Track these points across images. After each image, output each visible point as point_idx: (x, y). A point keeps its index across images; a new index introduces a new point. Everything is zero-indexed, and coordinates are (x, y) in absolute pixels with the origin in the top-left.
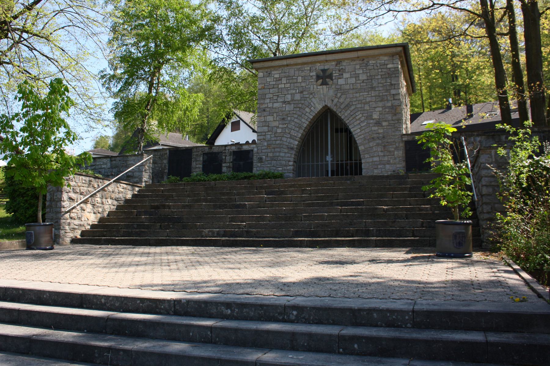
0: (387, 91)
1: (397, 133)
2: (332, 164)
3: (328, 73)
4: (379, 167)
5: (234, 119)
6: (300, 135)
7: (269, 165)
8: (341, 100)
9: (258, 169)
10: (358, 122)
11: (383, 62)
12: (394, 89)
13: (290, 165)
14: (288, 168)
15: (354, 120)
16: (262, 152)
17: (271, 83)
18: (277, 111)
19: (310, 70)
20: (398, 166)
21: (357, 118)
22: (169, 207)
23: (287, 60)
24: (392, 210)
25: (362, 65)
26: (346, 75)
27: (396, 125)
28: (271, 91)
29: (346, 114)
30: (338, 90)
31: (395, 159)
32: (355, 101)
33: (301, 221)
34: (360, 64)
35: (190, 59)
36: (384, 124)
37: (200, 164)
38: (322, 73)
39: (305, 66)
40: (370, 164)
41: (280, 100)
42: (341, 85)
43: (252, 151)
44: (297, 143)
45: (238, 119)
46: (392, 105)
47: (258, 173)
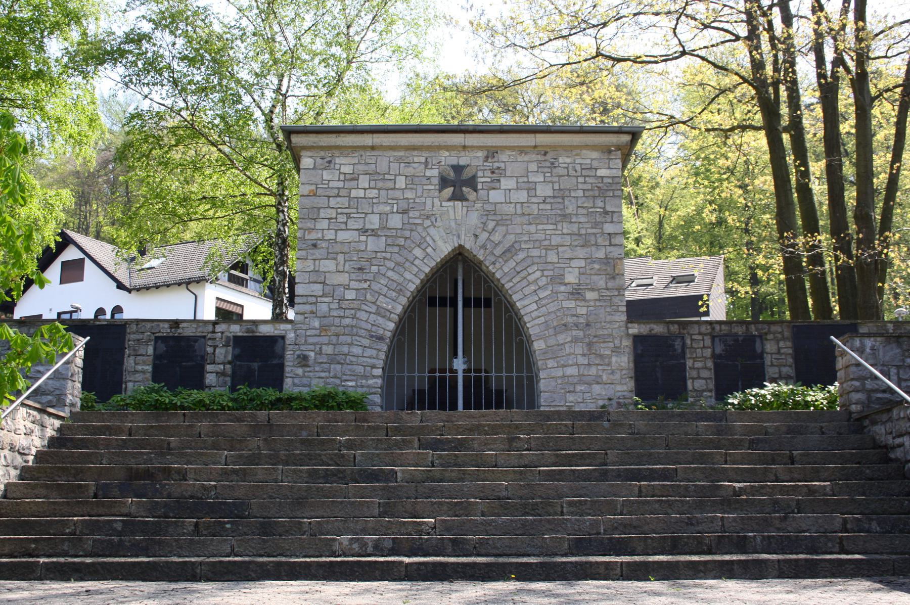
0: (596, 224)
2: (466, 380)
3: (467, 174)
4: (579, 388)
5: (71, 254)
6: (399, 309)
7: (323, 375)
8: (496, 237)
9: (296, 381)
10: (533, 287)
11: (589, 161)
12: (612, 222)
13: (374, 377)
14: (371, 382)
15: (525, 283)
16: (306, 343)
17: (332, 184)
18: (346, 249)
19: (426, 163)
20: (619, 388)
21: (531, 278)
22: (183, 475)
23: (375, 135)
24: (753, 491)
25: (544, 164)
26: (506, 183)
31: (613, 373)
33: (562, 514)
34: (539, 162)
35: (53, 106)
36: (590, 295)
37: (144, 363)
38: (452, 174)
39: (415, 153)
40: (559, 381)
41: (352, 224)
43: (283, 338)
44: (391, 326)
45: (81, 256)
46: (606, 258)
47: (296, 390)
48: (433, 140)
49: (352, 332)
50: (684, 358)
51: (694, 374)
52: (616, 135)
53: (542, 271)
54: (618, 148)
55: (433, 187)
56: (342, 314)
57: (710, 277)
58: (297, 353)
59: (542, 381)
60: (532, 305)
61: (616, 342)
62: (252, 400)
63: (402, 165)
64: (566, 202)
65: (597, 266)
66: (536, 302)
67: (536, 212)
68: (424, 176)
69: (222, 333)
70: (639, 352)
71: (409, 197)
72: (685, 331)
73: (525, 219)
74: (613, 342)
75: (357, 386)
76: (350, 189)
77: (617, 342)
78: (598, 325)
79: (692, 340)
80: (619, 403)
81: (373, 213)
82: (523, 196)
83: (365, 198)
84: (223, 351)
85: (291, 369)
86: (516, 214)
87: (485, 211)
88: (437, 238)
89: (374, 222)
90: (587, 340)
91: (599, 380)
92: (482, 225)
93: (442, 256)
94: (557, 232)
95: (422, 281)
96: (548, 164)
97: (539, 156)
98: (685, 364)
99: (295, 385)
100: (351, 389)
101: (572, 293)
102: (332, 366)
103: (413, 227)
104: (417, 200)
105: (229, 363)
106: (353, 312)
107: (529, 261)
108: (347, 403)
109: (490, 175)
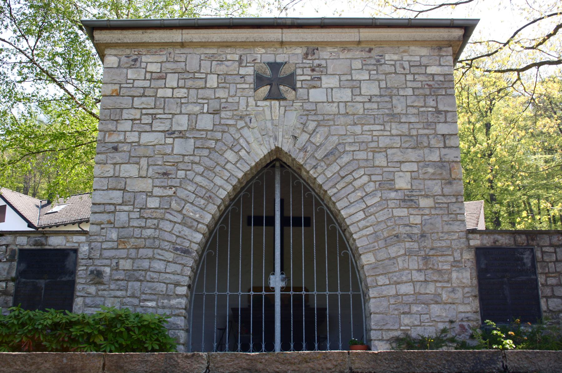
0: (428, 125)
1: (455, 228)
2: (285, 300)
3: (284, 72)
4: (415, 309)
6: (208, 218)
7: (119, 293)
8: (318, 139)
9: (88, 301)
10: (360, 194)
11: (418, 58)
12: (446, 122)
13: (178, 296)
14: (174, 302)
15: (350, 189)
16: (101, 257)
17: (136, 84)
18: (149, 152)
19: (240, 61)
20: (461, 308)
21: (357, 183)
23: (185, 31)
25: (368, 62)
26: (327, 82)
27: (454, 207)
28: (137, 102)
29: (329, 174)
30: (307, 113)
31: (453, 291)
32: (350, 144)
34: (364, 59)
36: (424, 202)
39: (229, 50)
40: (392, 301)
41: (157, 125)
42: (316, 103)
43: (75, 251)
44: (199, 237)
45: (4, 203)
46: (441, 161)
47: (89, 311)
48: (248, 35)
49: (154, 243)
50: (535, 273)
51: (548, 292)
53: (370, 175)
54: (449, 43)
55: (247, 86)
56: (143, 224)
57: (476, 216)
58: (91, 268)
59: (372, 301)
60: (360, 214)
62: (23, 325)
63: (214, 63)
64: (394, 101)
65: (431, 170)
66: (363, 210)
67: (361, 111)
68: (238, 74)
69: (7, 246)
70: (483, 266)
71: (221, 96)
73: (349, 119)
74: (452, 255)
75: (158, 307)
76: (157, 89)
77: (457, 255)
78: (435, 236)
79: (543, 253)
80: (462, 327)
81: (181, 113)
82: (346, 95)
83: (172, 97)
85: (83, 285)
86: (339, 114)
87: (304, 110)
88: (251, 140)
89: (182, 123)
90: (423, 253)
91: (438, 299)
92: (301, 126)
93: (258, 160)
95: (234, 187)
96: (373, 62)
97: (363, 53)
98: (536, 280)
99: (86, 305)
101: (404, 201)
102: (130, 284)
103: (225, 128)
104: (230, 100)
105: (13, 280)
106: (156, 222)
107: (354, 165)
109: (310, 73)
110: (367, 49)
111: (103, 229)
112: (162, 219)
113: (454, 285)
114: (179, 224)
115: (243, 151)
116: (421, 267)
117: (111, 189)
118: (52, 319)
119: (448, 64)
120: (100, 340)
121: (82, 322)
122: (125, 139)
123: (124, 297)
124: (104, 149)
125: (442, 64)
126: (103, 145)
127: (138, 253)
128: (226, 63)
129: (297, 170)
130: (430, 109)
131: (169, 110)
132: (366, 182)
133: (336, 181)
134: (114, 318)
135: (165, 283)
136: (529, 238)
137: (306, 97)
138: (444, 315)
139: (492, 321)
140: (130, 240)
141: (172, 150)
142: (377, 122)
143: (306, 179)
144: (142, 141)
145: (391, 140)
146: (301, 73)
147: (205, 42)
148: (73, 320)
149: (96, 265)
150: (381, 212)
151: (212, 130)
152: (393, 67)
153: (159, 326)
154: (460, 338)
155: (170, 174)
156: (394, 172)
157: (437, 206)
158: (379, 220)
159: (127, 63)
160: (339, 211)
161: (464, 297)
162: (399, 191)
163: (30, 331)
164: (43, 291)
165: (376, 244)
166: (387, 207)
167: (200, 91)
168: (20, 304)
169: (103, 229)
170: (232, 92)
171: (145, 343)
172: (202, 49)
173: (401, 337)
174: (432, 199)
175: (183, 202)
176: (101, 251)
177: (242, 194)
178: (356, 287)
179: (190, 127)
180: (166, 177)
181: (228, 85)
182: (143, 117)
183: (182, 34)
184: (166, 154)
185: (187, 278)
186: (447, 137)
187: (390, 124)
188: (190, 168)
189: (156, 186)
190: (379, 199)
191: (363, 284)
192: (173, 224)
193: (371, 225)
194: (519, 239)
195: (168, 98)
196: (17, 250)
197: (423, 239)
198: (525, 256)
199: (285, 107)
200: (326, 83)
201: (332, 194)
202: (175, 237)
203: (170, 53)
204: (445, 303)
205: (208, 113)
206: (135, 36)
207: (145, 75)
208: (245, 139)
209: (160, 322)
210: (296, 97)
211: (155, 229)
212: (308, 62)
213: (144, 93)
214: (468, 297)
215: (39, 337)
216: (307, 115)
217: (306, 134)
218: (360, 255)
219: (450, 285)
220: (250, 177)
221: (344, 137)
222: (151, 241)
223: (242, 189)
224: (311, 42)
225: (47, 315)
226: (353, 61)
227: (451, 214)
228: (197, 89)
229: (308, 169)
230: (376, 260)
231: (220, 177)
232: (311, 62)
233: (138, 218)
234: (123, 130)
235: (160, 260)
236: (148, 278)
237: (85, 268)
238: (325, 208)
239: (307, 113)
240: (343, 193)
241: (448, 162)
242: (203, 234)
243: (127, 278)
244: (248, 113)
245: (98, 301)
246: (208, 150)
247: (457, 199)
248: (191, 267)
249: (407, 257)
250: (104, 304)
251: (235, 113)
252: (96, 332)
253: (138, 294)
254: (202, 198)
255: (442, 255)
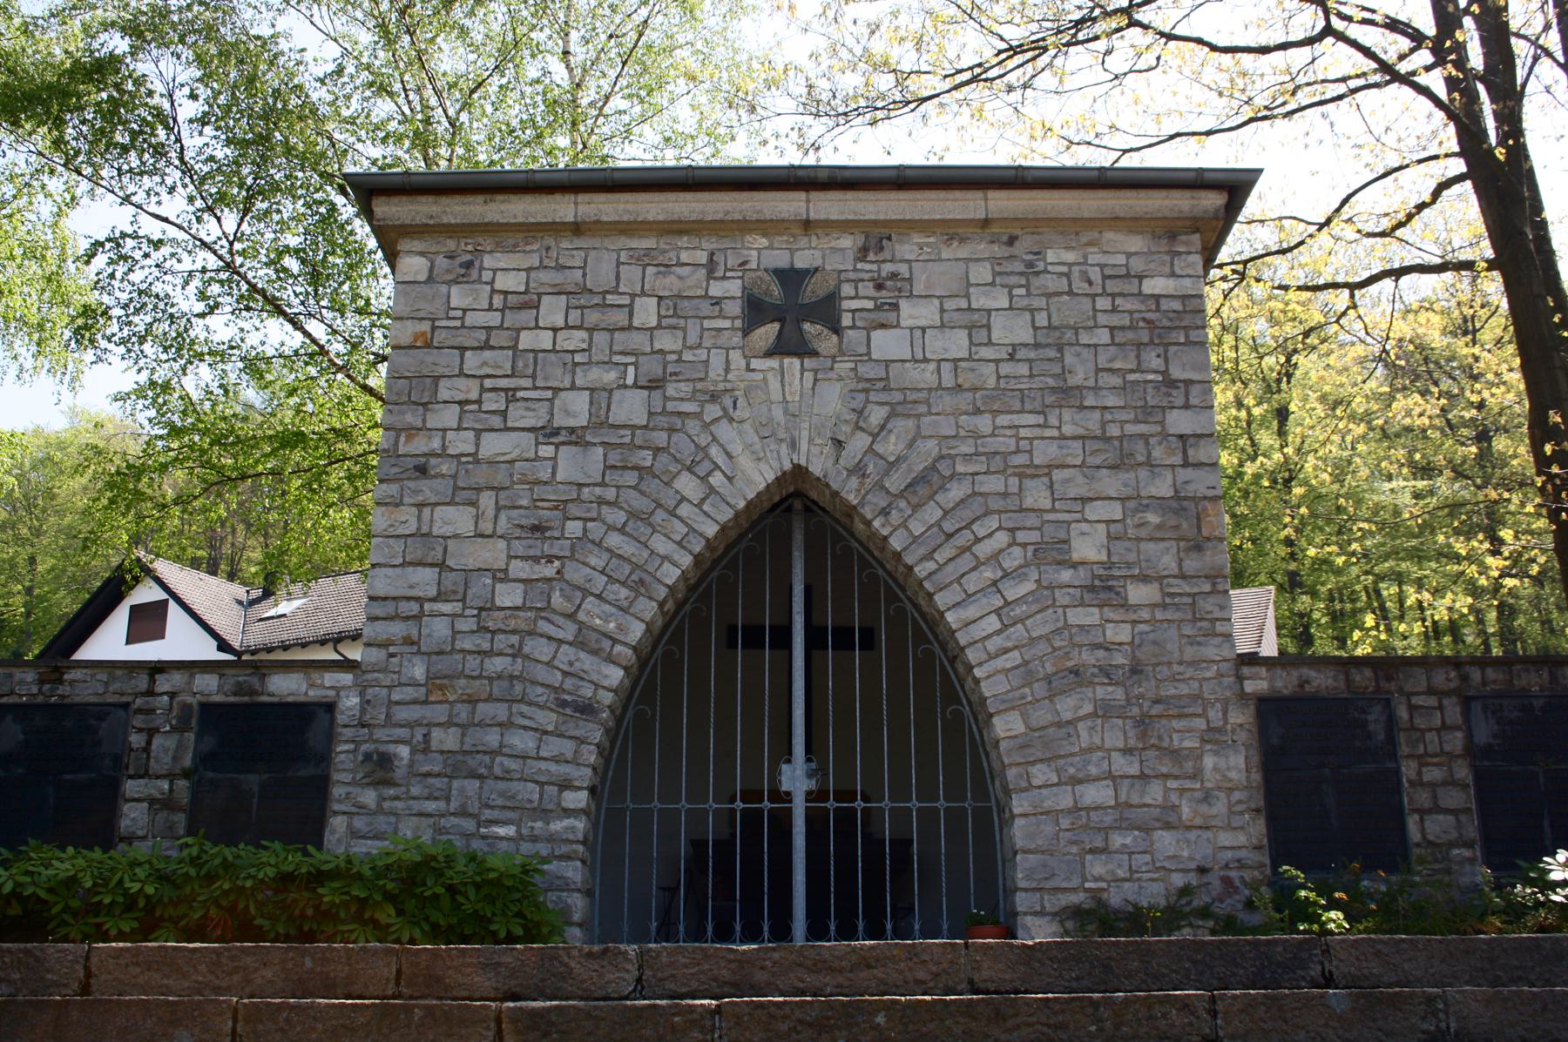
0: (1146, 413)
1: (1210, 652)
3: (813, 290)
4: (1117, 840)
5: (146, 593)
6: (636, 631)
7: (431, 806)
8: (891, 446)
9: (359, 823)
10: (989, 574)
11: (1121, 259)
12: (1187, 406)
13: (568, 813)
14: (557, 826)
15: (966, 561)
16: (389, 722)
17: (471, 319)
18: (501, 478)
19: (711, 266)
20: (1225, 839)
21: (983, 550)
23: (582, 197)
26: (913, 313)
27: (1207, 605)
28: (472, 361)
29: (917, 528)
30: (867, 386)
31: (1207, 798)
32: (967, 457)
34: (996, 261)
36: (1138, 593)
38: (776, 290)
39: (684, 241)
40: (1065, 823)
41: (520, 416)
42: (888, 363)
44: (615, 675)
45: (164, 596)
46: (1177, 497)
47: (361, 848)
48: (728, 206)
49: (512, 689)
50: (1394, 756)
51: (1423, 798)
52: (1188, 194)
53: (1012, 530)
54: (1195, 224)
55: (727, 324)
56: (486, 646)
58: (364, 747)
59: (1019, 822)
60: (989, 621)
61: (1211, 714)
64: (1069, 359)
65: (1153, 518)
66: (997, 612)
67: (992, 382)
68: (706, 296)
69: (172, 695)
70: (1275, 741)
71: (667, 348)
72: (1393, 686)
74: (1204, 715)
75: (521, 837)
76: (518, 331)
78: (1164, 671)
79: (1412, 708)
80: (1227, 881)
81: (573, 387)
82: (957, 345)
83: (554, 351)
84: (171, 742)
86: (940, 387)
87: (860, 380)
88: (736, 448)
89: (576, 409)
90: (1135, 711)
91: (1172, 819)
92: (853, 416)
93: (751, 496)
94: (1048, 433)
95: (698, 558)
98: (1397, 772)
99: (354, 834)
100: (504, 845)
101: (1091, 589)
102: (456, 784)
104: (687, 356)
105: (186, 774)
106: (515, 639)
107: (976, 507)
108: (478, 886)
109: (872, 292)
110: (1005, 238)
111: (392, 655)
112: (531, 633)
113: (1209, 785)
114: (570, 644)
115: (718, 474)
116: (1132, 743)
117: (411, 564)
118: (276, 866)
119: (1191, 272)
120: (386, 915)
121: (345, 873)
122: (444, 447)
123: (443, 816)
124: (394, 470)
125: (1178, 272)
126: (393, 461)
127: (473, 713)
128: (677, 269)
129: (843, 520)
130: (1151, 377)
131: (546, 379)
132: (1004, 546)
133: (933, 544)
134: (418, 864)
135: (536, 782)
136: (1380, 673)
137: (863, 350)
138: (1185, 854)
139: (1297, 869)
140: (455, 682)
141: (554, 474)
142: (1028, 407)
143: (865, 540)
144: (484, 453)
145: (1060, 447)
146: (853, 293)
147: (629, 223)
148: (325, 867)
149: (376, 741)
150: (1039, 616)
151: (645, 427)
152: (1065, 280)
153: (522, 882)
154: (1222, 909)
155: (550, 528)
156: (1069, 523)
157: (1168, 600)
158: (1034, 635)
159: (448, 271)
160: (942, 614)
161: (1231, 812)
162: (1080, 568)
163: (226, 893)
164: (255, 800)
165: (1027, 690)
166: (1053, 605)
167: (617, 334)
168: (202, 831)
169: (392, 655)
170: (693, 338)
171: (490, 921)
172: (623, 238)
173: (1086, 906)
174: (1156, 585)
175: (579, 594)
176: (388, 707)
177: (715, 574)
178: (982, 792)
179: (594, 419)
180: (538, 535)
181: (682, 322)
182: (485, 396)
183: (576, 204)
184: (538, 482)
185: (589, 771)
186: (1192, 441)
187: (1057, 411)
188: (595, 515)
189: (516, 557)
190: (1034, 586)
191: (997, 783)
192: (555, 644)
193: (1016, 647)
194: (1358, 678)
195: (544, 351)
196: (196, 707)
197: (1135, 677)
198: (1371, 718)
199: (816, 371)
200: (911, 317)
201: (924, 574)
202: (559, 675)
203: (548, 249)
204: (1189, 828)
205: (636, 386)
206: (467, 208)
207: (491, 298)
208: (721, 445)
209: (526, 872)
210: (840, 349)
211: (514, 656)
212: (868, 267)
213: (488, 340)
214: (1241, 813)
215: (247, 907)
216: (867, 391)
217: (865, 436)
218: (991, 716)
219: (1198, 786)
220: (733, 534)
221: (952, 442)
222: (505, 684)
223: (716, 562)
224: (876, 223)
225: (264, 856)
226: (971, 265)
227: (1201, 619)
228: (612, 331)
229: (869, 517)
230: (1027, 727)
231: (665, 535)
232: (874, 267)
233: (473, 632)
234: (439, 426)
235: (525, 728)
236: (497, 771)
237: (352, 746)
238: (909, 606)
239: (867, 385)
240: (951, 572)
241: (1193, 498)
242: (626, 668)
243: (449, 771)
244: (729, 386)
245: (382, 823)
246: (636, 473)
247: (1214, 585)
248: (598, 745)
249: (1099, 721)
250: (396, 831)
251: (699, 386)
252: (378, 897)
253: (474, 807)
254: (623, 584)
255: (1180, 716)
